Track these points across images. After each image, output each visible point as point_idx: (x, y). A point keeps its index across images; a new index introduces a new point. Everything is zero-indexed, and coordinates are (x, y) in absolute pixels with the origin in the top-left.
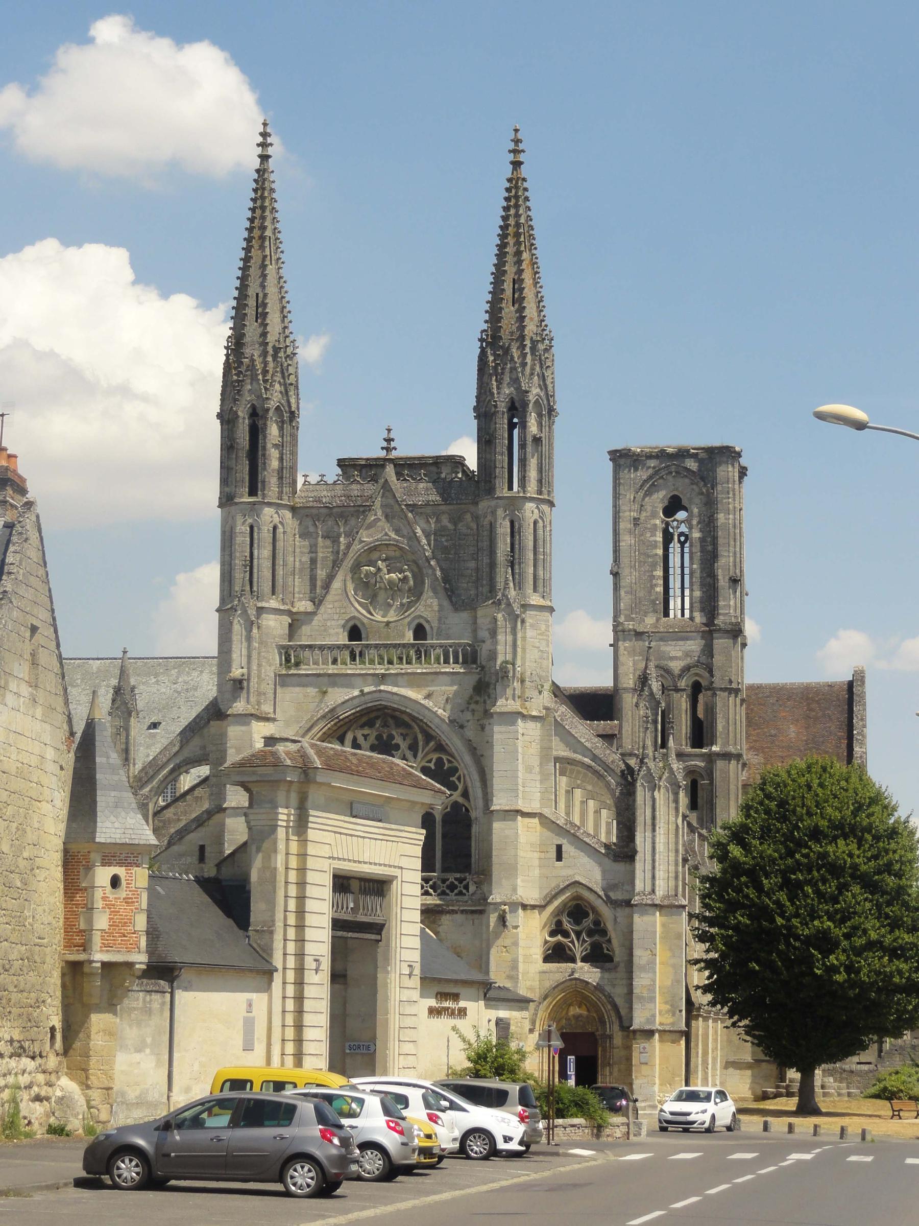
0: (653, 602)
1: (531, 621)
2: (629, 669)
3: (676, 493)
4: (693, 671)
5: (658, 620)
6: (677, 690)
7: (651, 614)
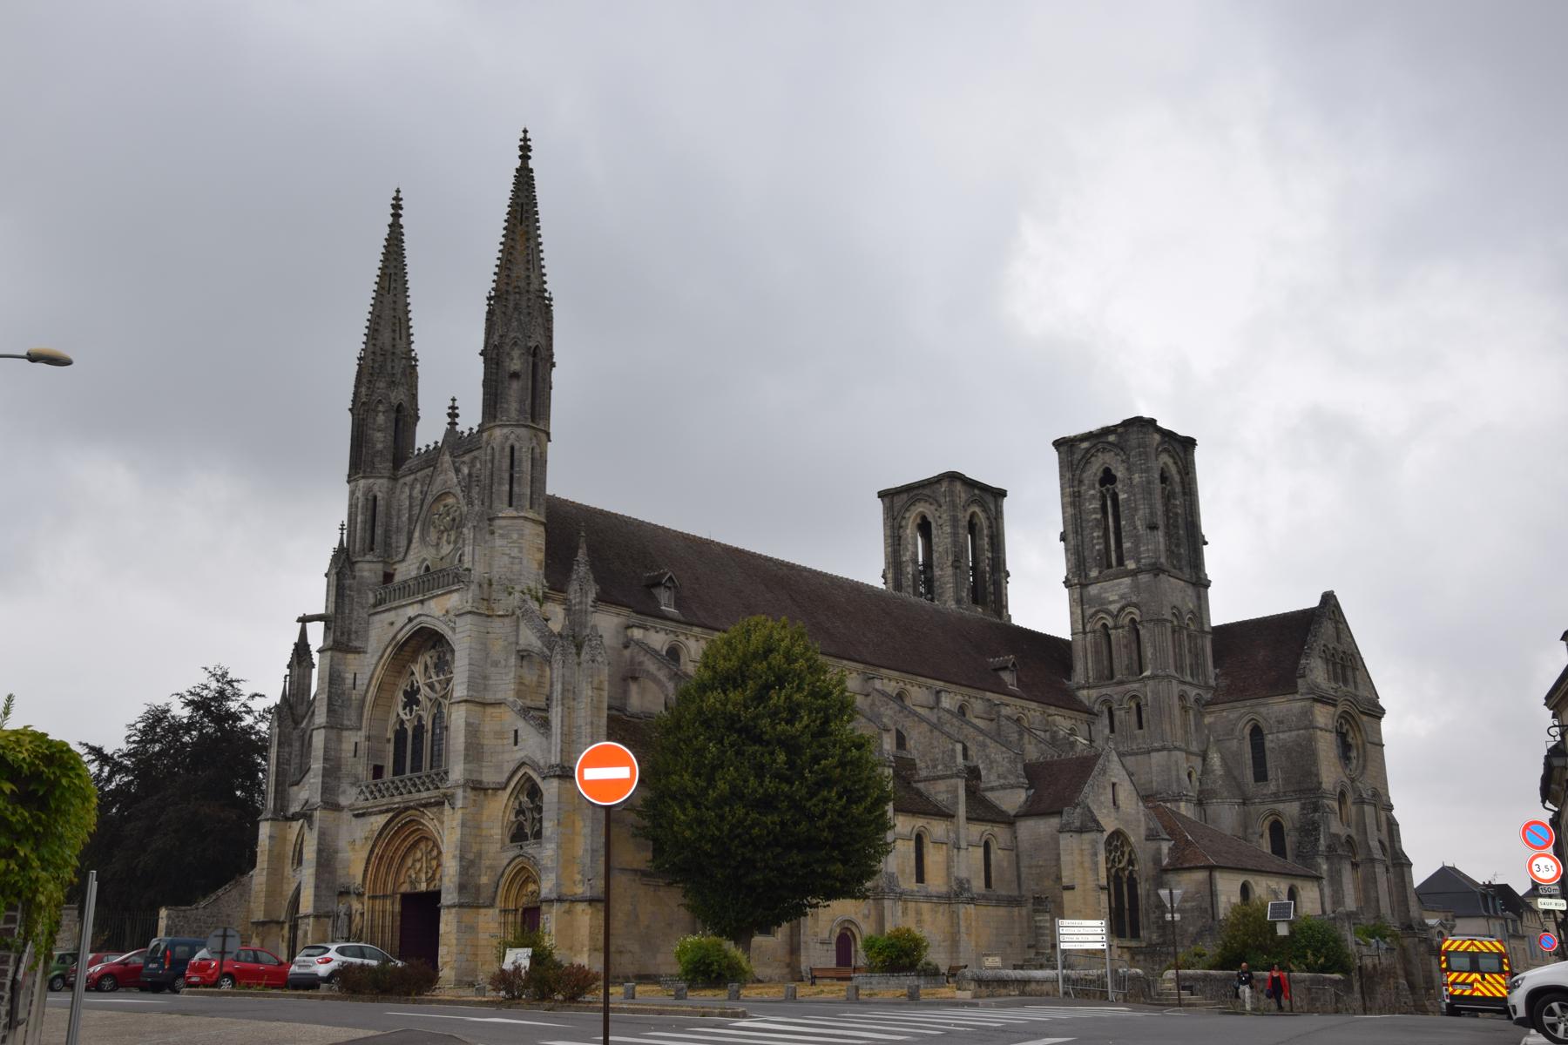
1: (501, 532)
5: (1100, 572)
6: (1116, 627)
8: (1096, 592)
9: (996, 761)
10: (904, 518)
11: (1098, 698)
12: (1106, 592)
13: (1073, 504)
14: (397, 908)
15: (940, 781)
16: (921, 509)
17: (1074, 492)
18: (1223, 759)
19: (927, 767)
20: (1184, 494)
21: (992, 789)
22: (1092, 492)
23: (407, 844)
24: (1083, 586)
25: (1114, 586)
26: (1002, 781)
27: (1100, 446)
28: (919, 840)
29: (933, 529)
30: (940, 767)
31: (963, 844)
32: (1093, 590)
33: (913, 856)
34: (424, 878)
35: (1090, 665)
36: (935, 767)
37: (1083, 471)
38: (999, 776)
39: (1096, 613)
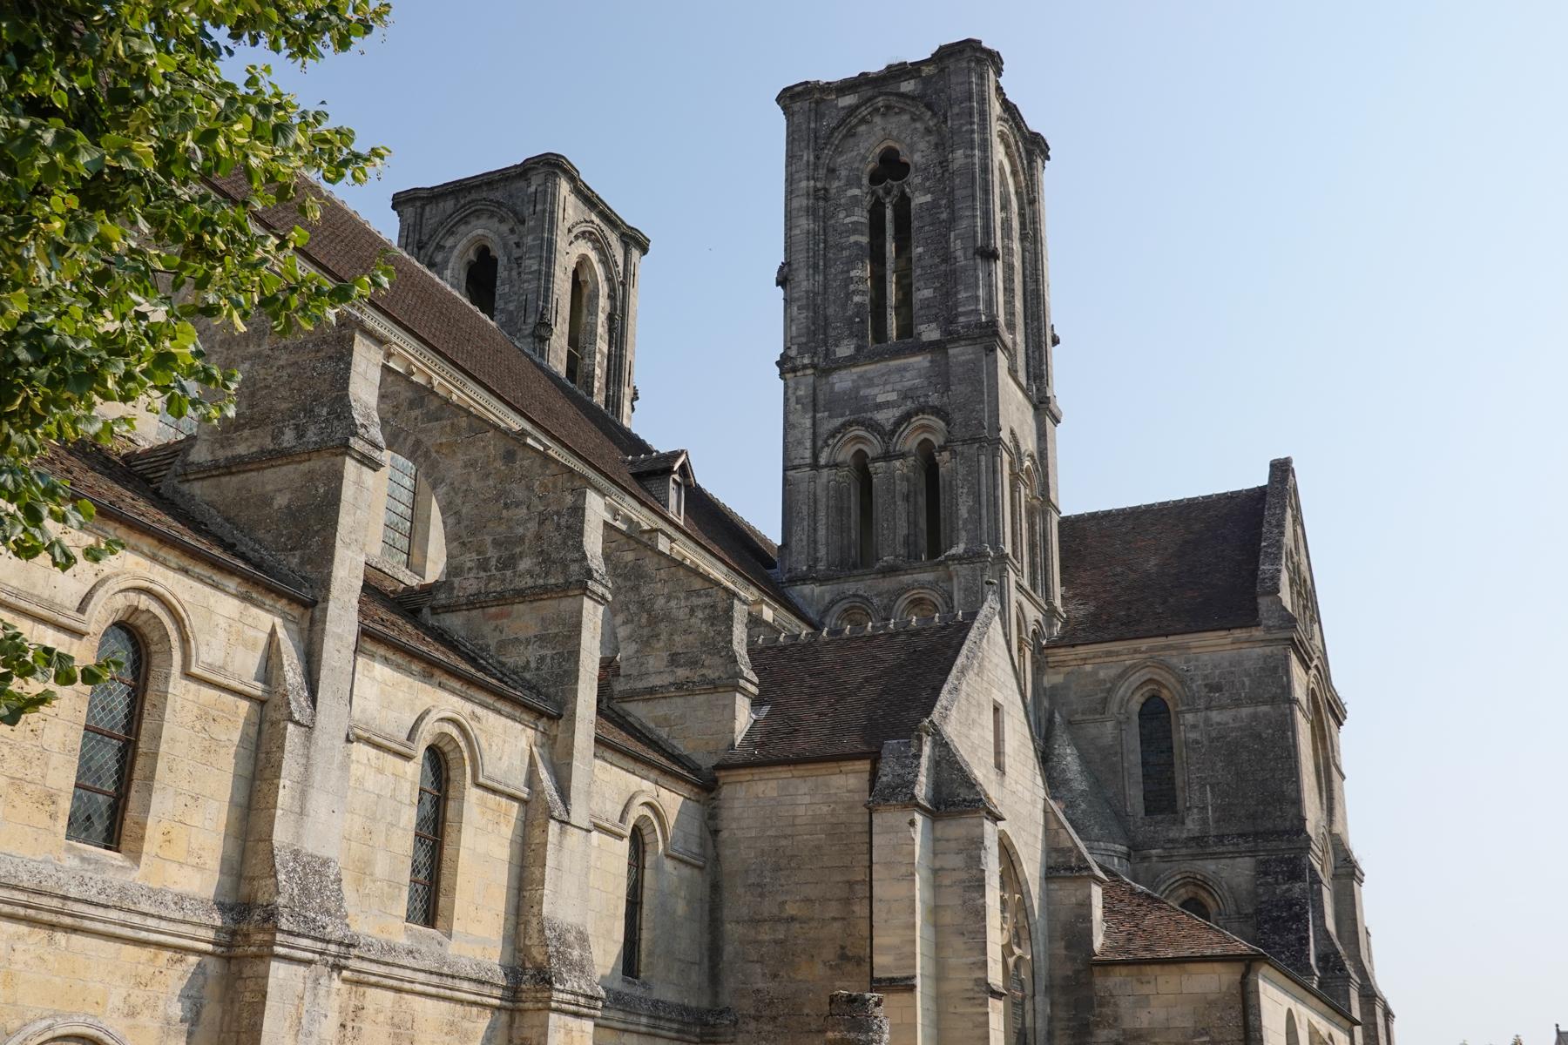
0: (850, 321)
2: (803, 433)
3: (891, 143)
4: (917, 421)
6: (887, 456)
7: (846, 342)
8: (848, 384)
9: (668, 617)
10: (440, 247)
11: (833, 603)
12: (870, 383)
13: (811, 212)
15: (520, 608)
16: (480, 231)
17: (816, 190)
18: (1084, 758)
19: (483, 565)
20: (1023, 238)
21: (651, 693)
22: (856, 192)
24: (824, 371)
25: (890, 373)
26: (682, 673)
27: (880, 101)
28: (439, 762)
29: (500, 269)
30: (525, 564)
31: (579, 815)
32: (842, 381)
33: (409, 817)
35: (822, 532)
36: (509, 563)
37: (838, 151)
38: (674, 660)
39: (850, 424)
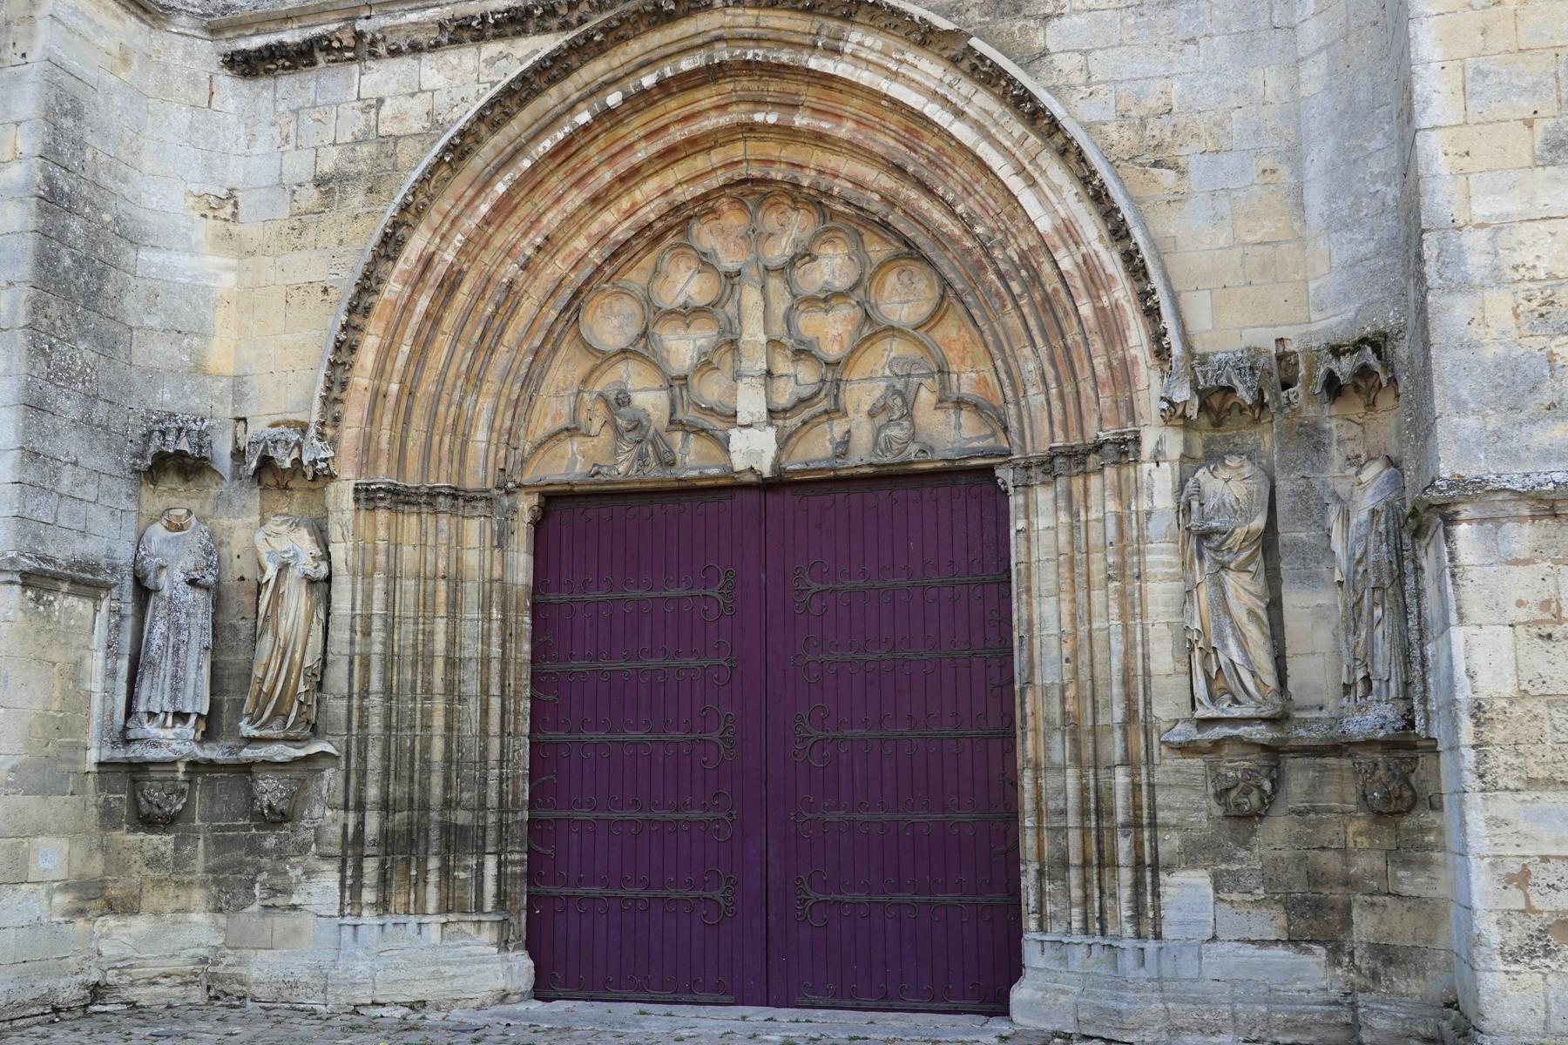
14: (520, 566)
23: (613, 221)
34: (750, 401)
